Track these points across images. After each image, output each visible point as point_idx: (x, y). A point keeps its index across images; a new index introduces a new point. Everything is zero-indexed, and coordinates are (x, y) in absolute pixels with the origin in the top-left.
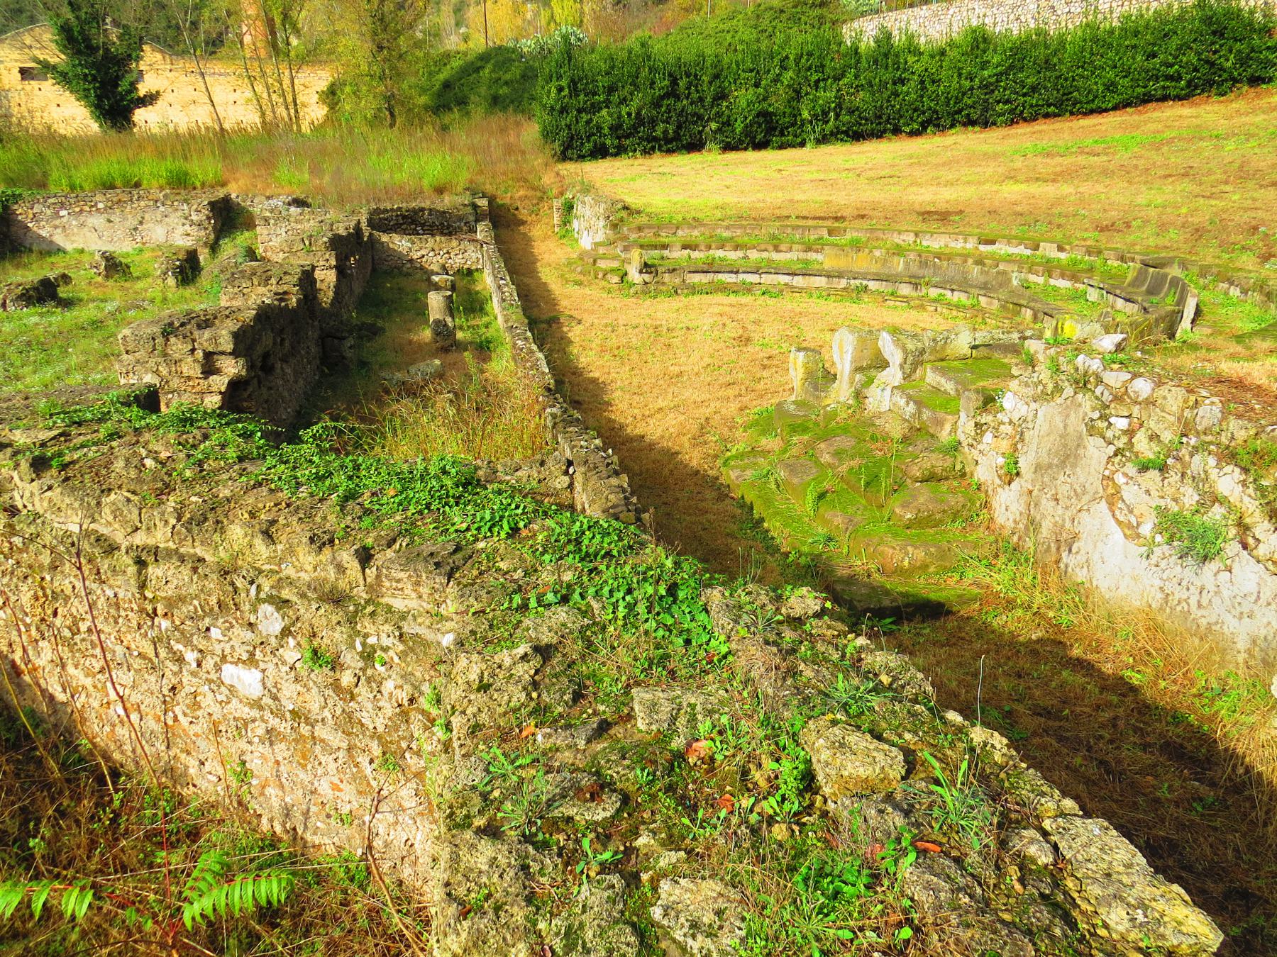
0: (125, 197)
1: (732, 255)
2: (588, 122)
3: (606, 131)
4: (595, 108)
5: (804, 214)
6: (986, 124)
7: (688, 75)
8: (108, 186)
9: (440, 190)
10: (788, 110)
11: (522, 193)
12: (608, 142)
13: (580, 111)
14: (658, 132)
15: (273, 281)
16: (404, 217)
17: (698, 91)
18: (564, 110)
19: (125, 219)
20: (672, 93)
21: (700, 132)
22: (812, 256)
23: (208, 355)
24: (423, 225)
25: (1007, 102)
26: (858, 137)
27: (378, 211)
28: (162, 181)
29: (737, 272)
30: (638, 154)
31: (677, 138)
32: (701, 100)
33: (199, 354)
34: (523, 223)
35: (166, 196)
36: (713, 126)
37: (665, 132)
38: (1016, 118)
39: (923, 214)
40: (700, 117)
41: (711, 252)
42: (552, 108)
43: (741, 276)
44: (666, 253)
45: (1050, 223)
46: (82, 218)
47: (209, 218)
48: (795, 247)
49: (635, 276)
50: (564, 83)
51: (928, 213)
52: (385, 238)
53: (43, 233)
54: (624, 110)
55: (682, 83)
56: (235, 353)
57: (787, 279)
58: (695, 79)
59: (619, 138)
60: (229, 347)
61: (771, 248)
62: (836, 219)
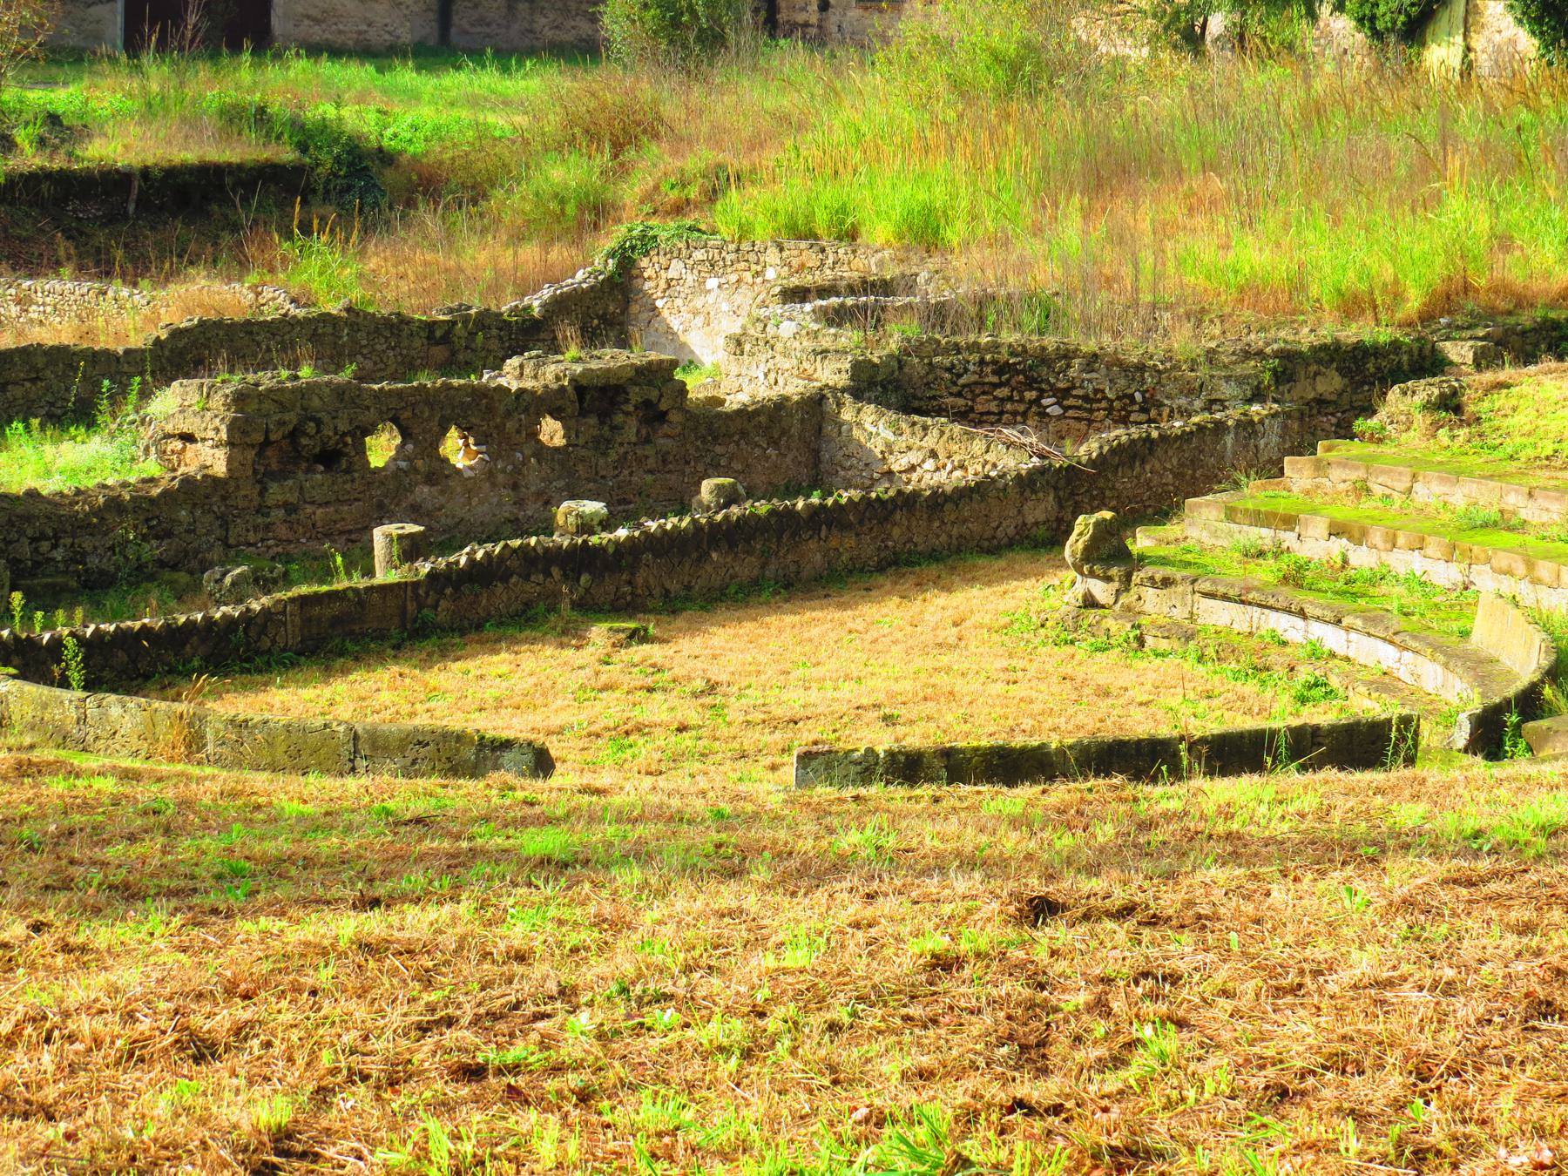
9: (1352, 306)
16: (1002, 369)
24: (1062, 395)
43: (1318, 630)
44: (1289, 538)
53: (675, 324)
61: (1521, 569)
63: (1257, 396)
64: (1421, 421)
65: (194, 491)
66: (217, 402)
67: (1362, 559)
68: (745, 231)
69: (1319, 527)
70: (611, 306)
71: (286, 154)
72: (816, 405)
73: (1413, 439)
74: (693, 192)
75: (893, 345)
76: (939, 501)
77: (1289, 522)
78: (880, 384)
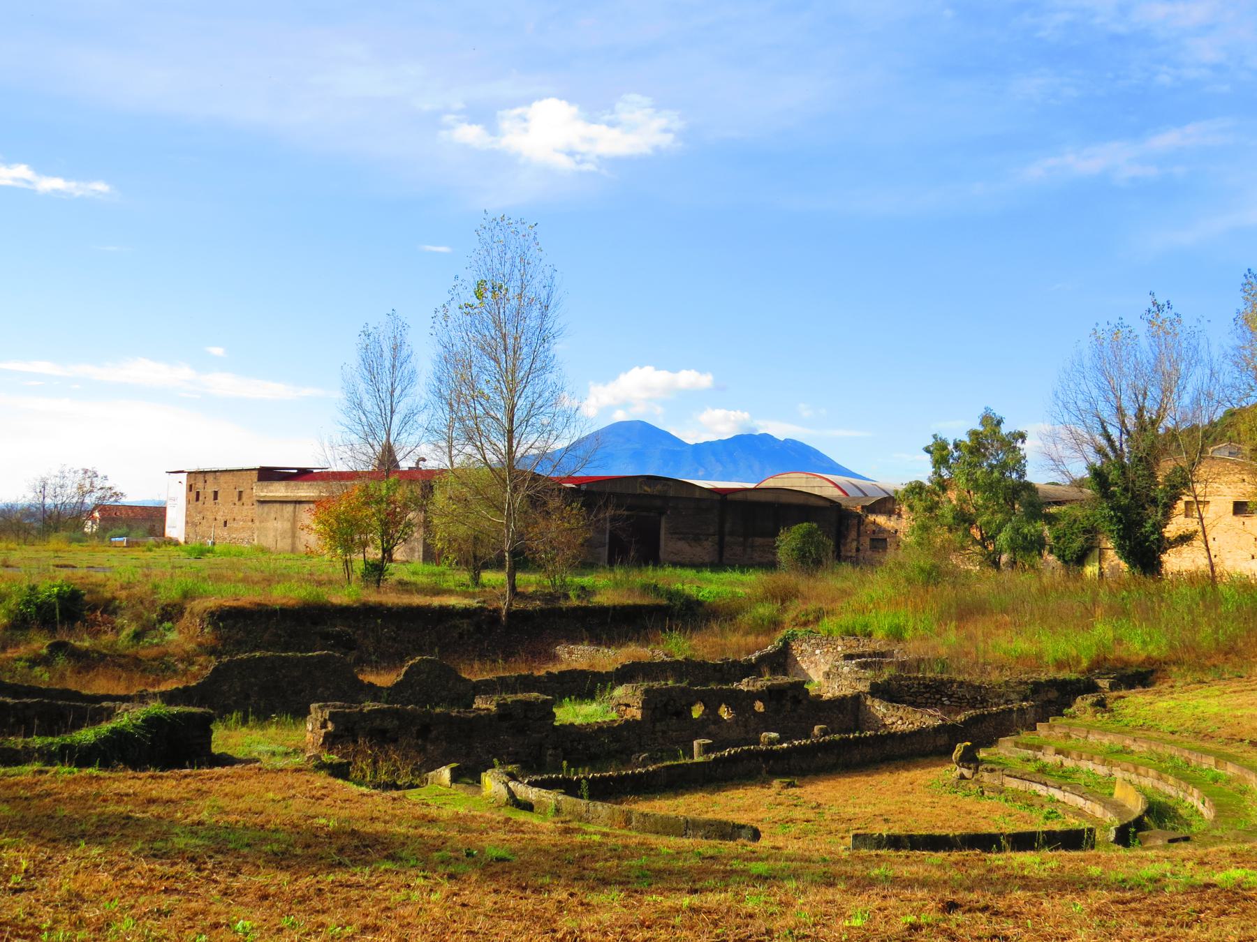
9: (1060, 665)
16: (926, 686)
43: (1052, 791)
44: (1040, 755)
53: (804, 667)
57: (1080, 802)
61: (1132, 769)
63: (1025, 699)
64: (1090, 710)
65: (630, 725)
66: (638, 693)
67: (1069, 763)
68: (830, 633)
69: (1051, 751)
70: (781, 659)
71: (665, 602)
72: (857, 699)
73: (1087, 717)
74: (811, 618)
75: (886, 677)
76: (904, 736)
77: (1039, 748)
78: (878, 691)
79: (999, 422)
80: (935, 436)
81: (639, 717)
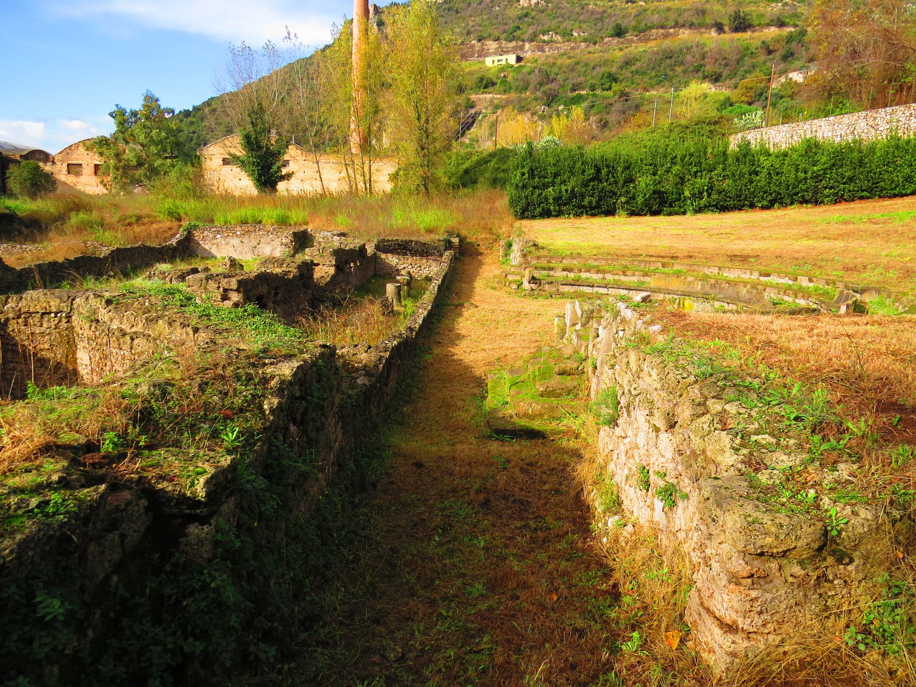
0: (252, 229)
1: (595, 277)
2: (540, 195)
3: (551, 201)
4: (545, 186)
5: (653, 253)
6: (817, 203)
7: (608, 167)
8: (244, 222)
9: (430, 231)
10: (675, 190)
11: (483, 236)
12: (552, 208)
13: (534, 188)
14: (586, 203)
15: (285, 265)
16: (399, 245)
17: (614, 177)
18: (524, 187)
19: (250, 241)
20: (597, 178)
21: (614, 203)
22: (647, 279)
23: (225, 290)
24: (410, 251)
25: (831, 188)
26: (724, 209)
27: (383, 241)
28: (273, 220)
29: (593, 286)
30: (571, 216)
31: (598, 206)
32: (616, 182)
33: (221, 289)
34: (481, 254)
35: (274, 229)
36: (623, 199)
37: (590, 202)
38: (838, 199)
39: (731, 256)
40: (615, 194)
41: (581, 274)
42: (517, 186)
43: (596, 289)
44: (552, 273)
45: (814, 265)
46: (228, 240)
47: (292, 241)
48: (637, 273)
49: (526, 286)
50: (526, 170)
51: (735, 256)
52: (383, 256)
53: (207, 247)
54: (563, 188)
55: (604, 171)
56: (238, 290)
58: (612, 169)
59: (559, 205)
60: (235, 287)
62: (672, 257)
74: (133, 220)
79: (157, 100)
80: (117, 105)
81: (332, 271)
